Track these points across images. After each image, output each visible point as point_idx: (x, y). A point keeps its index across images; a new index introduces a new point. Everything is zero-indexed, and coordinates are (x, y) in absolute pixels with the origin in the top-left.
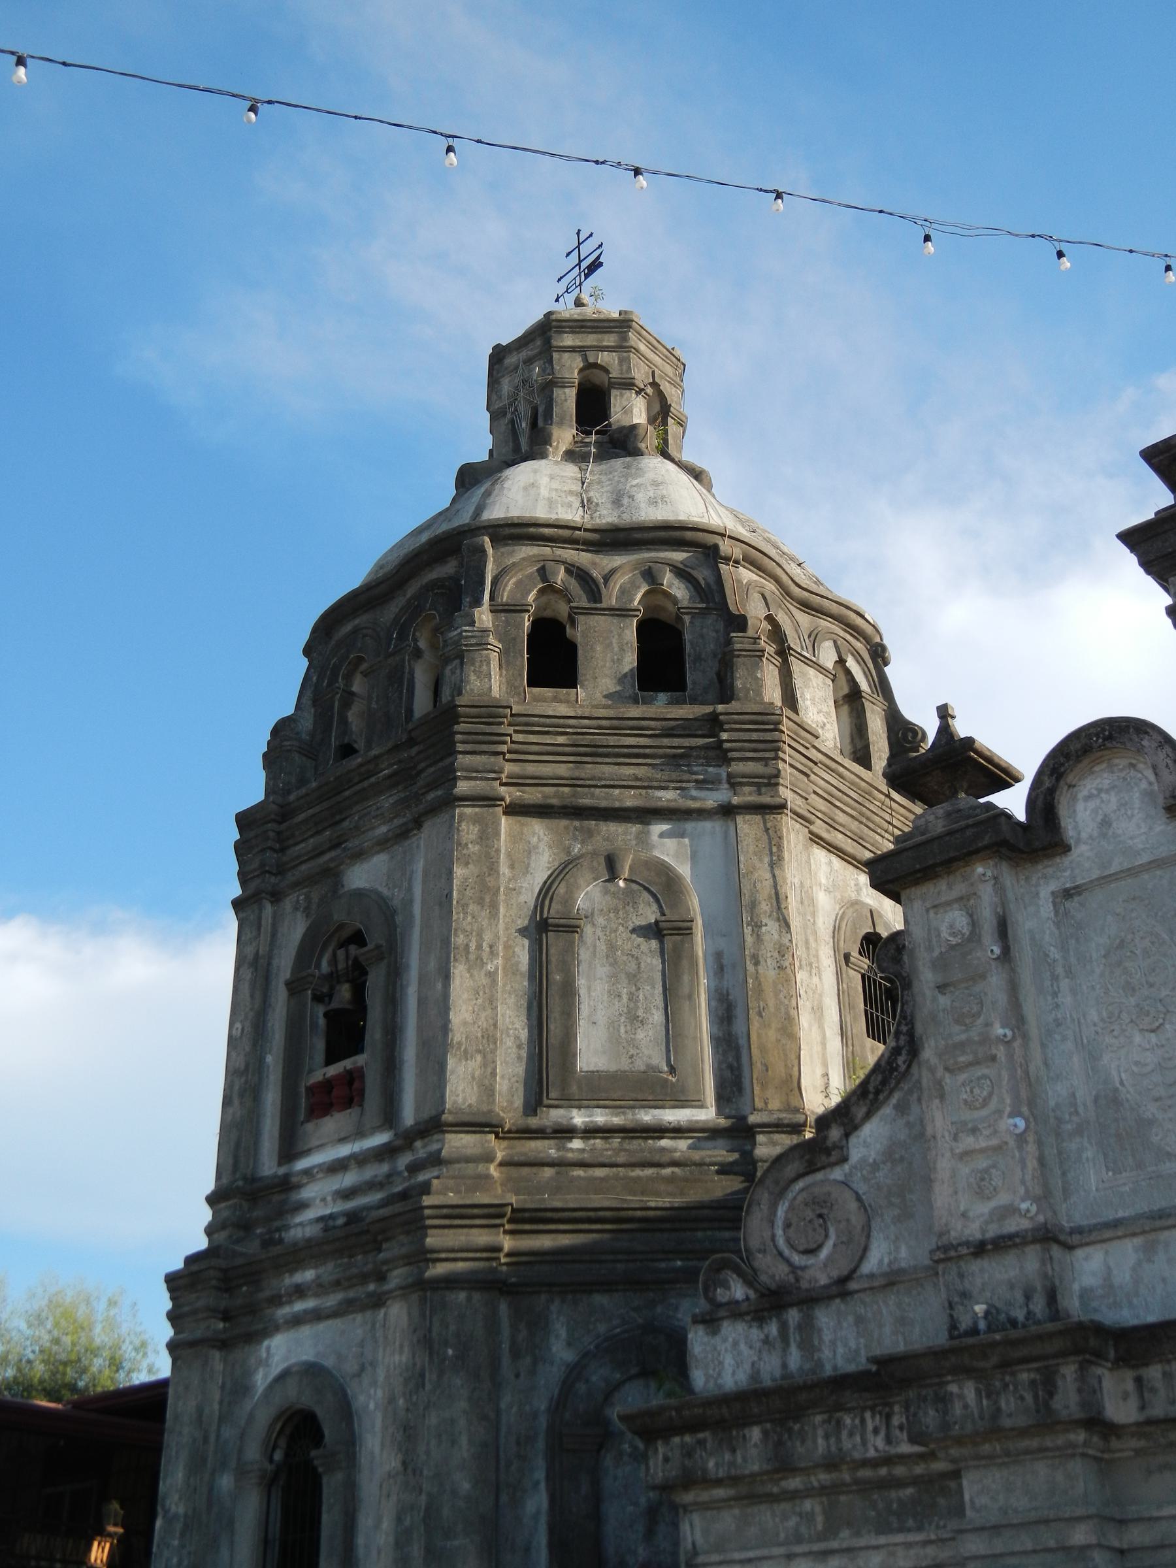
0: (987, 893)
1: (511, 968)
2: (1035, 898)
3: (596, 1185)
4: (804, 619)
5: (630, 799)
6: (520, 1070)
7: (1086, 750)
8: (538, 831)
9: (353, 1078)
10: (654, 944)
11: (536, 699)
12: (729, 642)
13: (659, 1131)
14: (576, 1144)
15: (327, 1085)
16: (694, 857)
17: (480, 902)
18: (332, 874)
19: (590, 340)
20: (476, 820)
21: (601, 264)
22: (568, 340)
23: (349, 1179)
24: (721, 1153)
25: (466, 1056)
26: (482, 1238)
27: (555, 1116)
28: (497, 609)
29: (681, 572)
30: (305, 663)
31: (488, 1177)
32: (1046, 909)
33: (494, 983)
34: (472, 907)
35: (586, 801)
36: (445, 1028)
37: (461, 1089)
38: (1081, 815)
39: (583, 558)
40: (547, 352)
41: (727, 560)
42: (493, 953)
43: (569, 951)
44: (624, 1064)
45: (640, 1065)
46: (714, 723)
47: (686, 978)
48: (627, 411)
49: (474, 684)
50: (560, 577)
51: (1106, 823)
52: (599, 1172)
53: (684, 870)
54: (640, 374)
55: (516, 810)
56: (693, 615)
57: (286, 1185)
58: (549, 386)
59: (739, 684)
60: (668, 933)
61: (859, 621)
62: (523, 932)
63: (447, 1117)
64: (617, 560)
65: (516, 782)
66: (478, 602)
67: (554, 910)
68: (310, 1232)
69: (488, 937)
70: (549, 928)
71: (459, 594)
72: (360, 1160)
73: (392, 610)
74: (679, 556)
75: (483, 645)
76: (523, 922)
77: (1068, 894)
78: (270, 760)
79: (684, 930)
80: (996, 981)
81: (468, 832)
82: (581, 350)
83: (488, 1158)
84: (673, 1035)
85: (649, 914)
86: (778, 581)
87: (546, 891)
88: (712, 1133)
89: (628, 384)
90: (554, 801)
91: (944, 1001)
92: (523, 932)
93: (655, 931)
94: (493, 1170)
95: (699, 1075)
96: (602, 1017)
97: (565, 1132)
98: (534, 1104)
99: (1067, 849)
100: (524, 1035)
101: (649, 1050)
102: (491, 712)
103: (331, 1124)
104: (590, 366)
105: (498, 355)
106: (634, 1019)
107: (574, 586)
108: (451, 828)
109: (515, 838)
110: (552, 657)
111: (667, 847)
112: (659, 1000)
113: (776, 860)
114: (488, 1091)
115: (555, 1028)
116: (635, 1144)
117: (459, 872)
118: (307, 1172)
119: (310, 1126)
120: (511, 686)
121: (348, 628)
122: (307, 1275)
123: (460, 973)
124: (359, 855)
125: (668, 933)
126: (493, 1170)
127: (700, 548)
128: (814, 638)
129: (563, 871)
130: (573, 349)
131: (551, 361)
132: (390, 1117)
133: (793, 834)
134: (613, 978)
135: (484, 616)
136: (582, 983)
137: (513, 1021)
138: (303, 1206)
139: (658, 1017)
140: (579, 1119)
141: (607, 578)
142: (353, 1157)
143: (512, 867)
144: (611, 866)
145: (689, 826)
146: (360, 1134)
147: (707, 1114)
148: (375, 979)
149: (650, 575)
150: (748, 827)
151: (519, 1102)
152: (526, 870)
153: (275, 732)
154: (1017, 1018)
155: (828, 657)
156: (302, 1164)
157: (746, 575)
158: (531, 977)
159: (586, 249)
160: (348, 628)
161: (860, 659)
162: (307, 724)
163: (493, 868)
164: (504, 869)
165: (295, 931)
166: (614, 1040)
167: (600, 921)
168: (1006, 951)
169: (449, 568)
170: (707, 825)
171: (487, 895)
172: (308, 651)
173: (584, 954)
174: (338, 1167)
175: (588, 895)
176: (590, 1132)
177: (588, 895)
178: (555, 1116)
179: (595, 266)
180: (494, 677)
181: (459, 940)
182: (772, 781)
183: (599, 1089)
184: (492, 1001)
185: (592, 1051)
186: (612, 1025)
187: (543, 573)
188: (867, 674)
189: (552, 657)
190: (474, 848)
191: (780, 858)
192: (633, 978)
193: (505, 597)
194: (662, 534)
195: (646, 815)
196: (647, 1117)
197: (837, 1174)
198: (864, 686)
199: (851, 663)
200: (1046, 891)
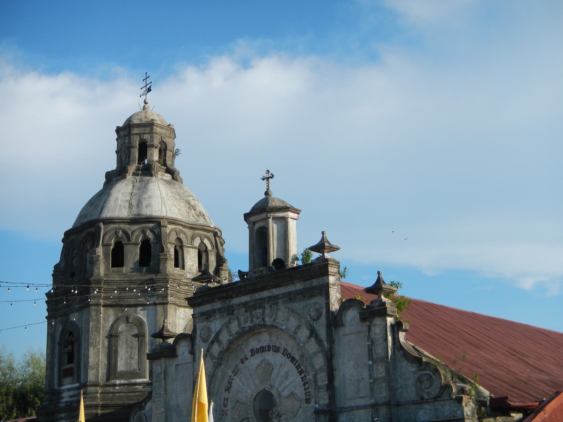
0: (163, 364)
1: (103, 347)
2: (172, 364)
3: (120, 398)
4: (189, 233)
5: (132, 302)
6: (105, 371)
7: (180, 339)
8: (111, 311)
9: (71, 369)
10: (137, 339)
11: (113, 272)
12: (159, 255)
13: (136, 384)
14: (117, 388)
15: (67, 370)
16: (148, 316)
17: (96, 331)
18: (66, 315)
19: (141, 130)
20: (96, 310)
21: (151, 90)
22: (136, 131)
23: (72, 393)
25: (93, 369)
26: (94, 411)
27: (113, 382)
28: (103, 245)
29: (152, 230)
30: (62, 244)
31: (97, 397)
32: (174, 368)
33: (99, 351)
34: (94, 333)
35: (121, 303)
36: (88, 362)
37: (91, 376)
39: (126, 227)
40: (129, 134)
41: (163, 227)
42: (99, 344)
43: (117, 342)
44: (128, 369)
45: (132, 369)
46: (152, 281)
47: (143, 347)
48: (152, 155)
49: (96, 271)
50: (120, 233)
51: (183, 353)
52: (122, 394)
53: (145, 320)
54: (156, 142)
55: (104, 306)
56: (154, 244)
57: (60, 392)
59: (161, 268)
60: (140, 336)
61: (209, 228)
62: (106, 337)
63: (88, 384)
64: (136, 227)
65: (105, 298)
66: (98, 246)
67: (113, 333)
68: (63, 405)
69: (98, 340)
70: (112, 336)
71: (94, 239)
72: (73, 389)
73: (82, 236)
74: (151, 225)
75: (98, 260)
76: (106, 335)
77: (177, 365)
78: (55, 276)
79: (143, 336)
80: (163, 382)
81: (93, 314)
83: (97, 393)
84: (140, 362)
85: (136, 331)
86: (181, 225)
87: (112, 326)
88: (147, 384)
89: (152, 146)
90: (114, 303)
91: (156, 384)
92: (106, 337)
93: (136, 336)
94: (98, 395)
95: (145, 371)
96: (124, 357)
97: (115, 385)
98: (108, 379)
99: (177, 356)
100: (106, 362)
101: (134, 365)
102: (99, 281)
103: (68, 380)
104: (141, 139)
106: (131, 358)
107: (124, 237)
108: (89, 313)
109: (105, 313)
110: (118, 259)
111: (142, 314)
112: (137, 353)
113: (166, 317)
114: (97, 377)
115: (113, 361)
116: (130, 387)
117: (91, 324)
118: (63, 390)
119: (64, 379)
120: (107, 268)
121: (71, 238)
122: (63, 415)
123: (91, 349)
124: (73, 312)
125: (140, 336)
126: (98, 395)
127: (157, 223)
128: (193, 238)
129: (116, 321)
130: (137, 134)
131: (130, 138)
132: (79, 381)
133: (171, 309)
134: (127, 347)
135: (100, 251)
136: (119, 349)
137: (103, 359)
138: (63, 398)
139: (136, 357)
140: (118, 382)
141: (132, 233)
142: (71, 388)
143: (104, 321)
144: (127, 319)
145: (147, 307)
146: (73, 383)
147: (147, 380)
148: (76, 346)
149: (144, 232)
150: (160, 308)
151: (105, 378)
152: (108, 321)
153: (55, 267)
154: (166, 390)
155: (197, 242)
156: (63, 388)
157: (170, 227)
158: (108, 349)
159: (148, 81)
160: (71, 238)
161: (209, 239)
162: (63, 265)
163: (99, 323)
164: (102, 321)
165: (60, 328)
166: (126, 363)
167: (124, 333)
168: (165, 378)
169: (93, 230)
170: (151, 307)
171: (97, 329)
172: (63, 241)
173: (120, 342)
174: (69, 390)
175: (122, 327)
176: (120, 385)
177: (122, 327)
178: (113, 382)
180: (102, 269)
181: (91, 341)
182: (165, 296)
183: (123, 375)
184: (98, 355)
185: (121, 366)
186: (126, 359)
187: (116, 233)
188: (211, 243)
189: (118, 259)
190: (94, 317)
191: (167, 316)
192: (131, 348)
193: (106, 242)
194: (146, 220)
195: (136, 306)
196: (133, 381)
197: (143, 412)
198: (209, 247)
199: (206, 241)
200: (175, 363)
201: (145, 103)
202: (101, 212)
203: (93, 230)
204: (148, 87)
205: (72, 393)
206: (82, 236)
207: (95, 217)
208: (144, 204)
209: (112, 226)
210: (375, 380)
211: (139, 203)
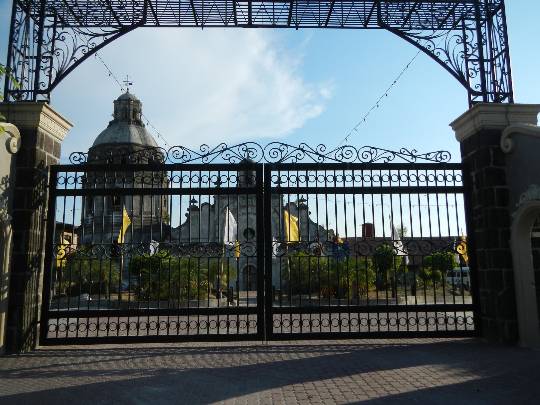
23: (118, 218)
24: (155, 220)
38: (204, 208)
40: (129, 104)
58: (130, 110)
73: (118, 148)
82: (134, 105)
105: (120, 99)
121: (109, 147)
160: (109, 147)
169: (127, 147)
179: (131, 84)
201: (128, 89)
202: (129, 139)
203: (127, 147)
204: (129, 82)
205: (118, 218)
206: (118, 148)
207: (127, 141)
208: (148, 140)
209: (137, 147)
210: (302, 229)
211: (145, 139)
